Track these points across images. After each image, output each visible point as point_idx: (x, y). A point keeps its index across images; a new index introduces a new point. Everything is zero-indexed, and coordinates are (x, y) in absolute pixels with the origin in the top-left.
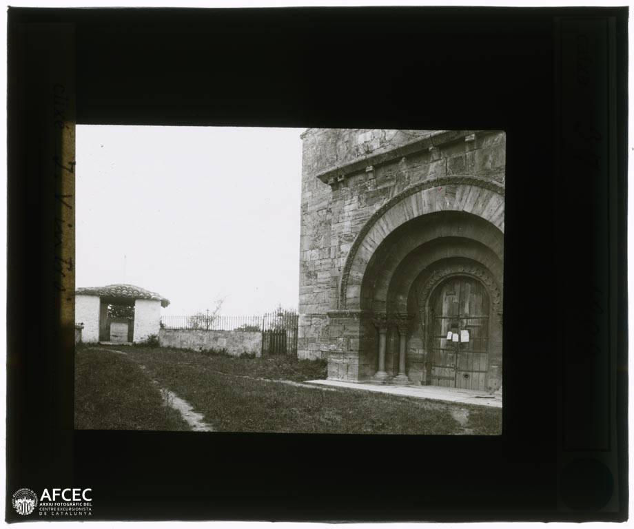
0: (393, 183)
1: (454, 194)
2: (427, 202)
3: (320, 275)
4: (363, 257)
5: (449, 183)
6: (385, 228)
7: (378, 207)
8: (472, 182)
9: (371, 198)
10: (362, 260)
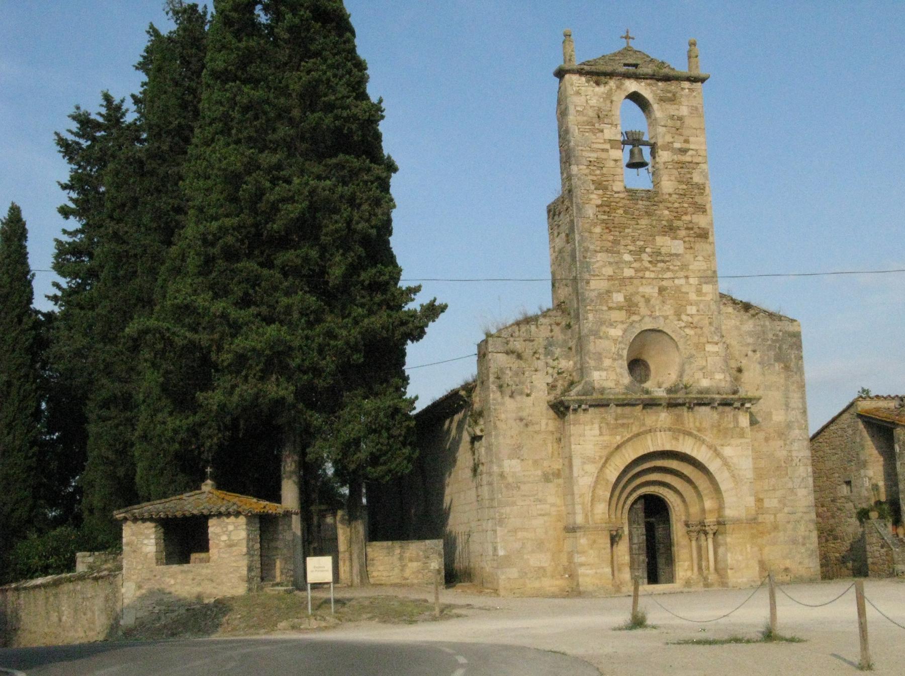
0: (632, 421)
1: (677, 439)
2: (663, 442)
3: (523, 487)
4: (609, 478)
5: (679, 431)
6: (627, 456)
7: (618, 439)
8: (690, 434)
9: (614, 429)
10: (608, 480)
